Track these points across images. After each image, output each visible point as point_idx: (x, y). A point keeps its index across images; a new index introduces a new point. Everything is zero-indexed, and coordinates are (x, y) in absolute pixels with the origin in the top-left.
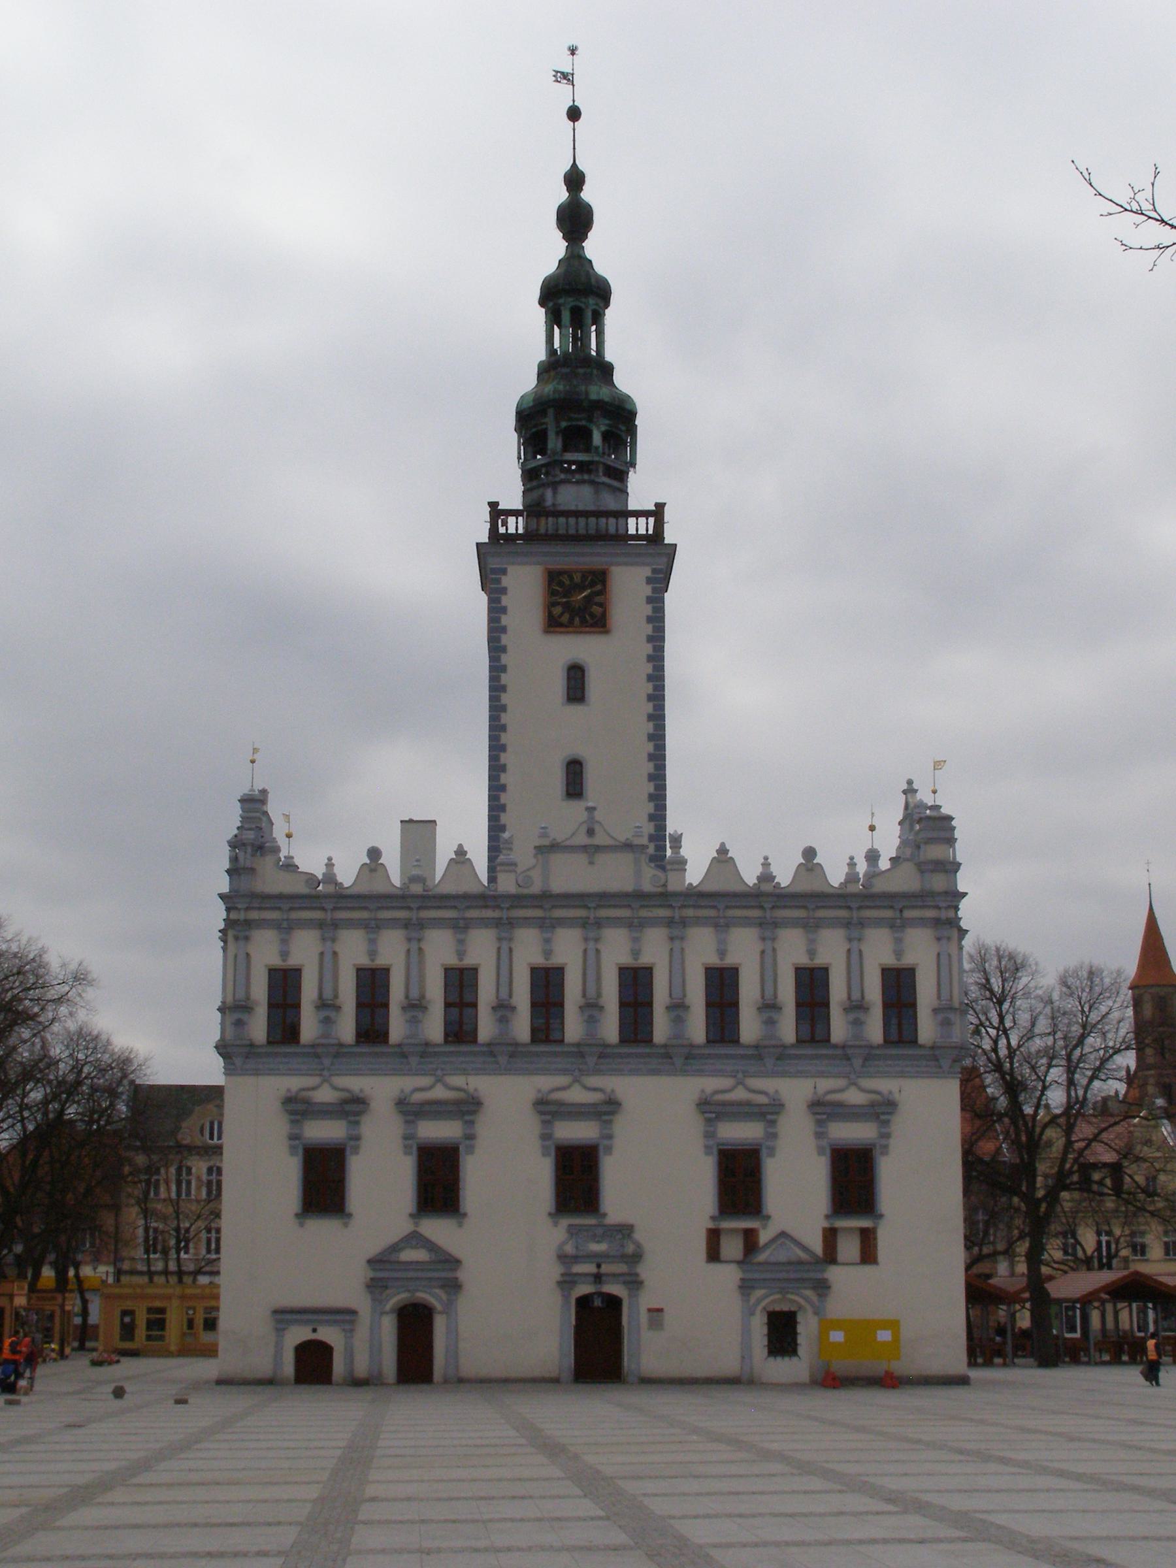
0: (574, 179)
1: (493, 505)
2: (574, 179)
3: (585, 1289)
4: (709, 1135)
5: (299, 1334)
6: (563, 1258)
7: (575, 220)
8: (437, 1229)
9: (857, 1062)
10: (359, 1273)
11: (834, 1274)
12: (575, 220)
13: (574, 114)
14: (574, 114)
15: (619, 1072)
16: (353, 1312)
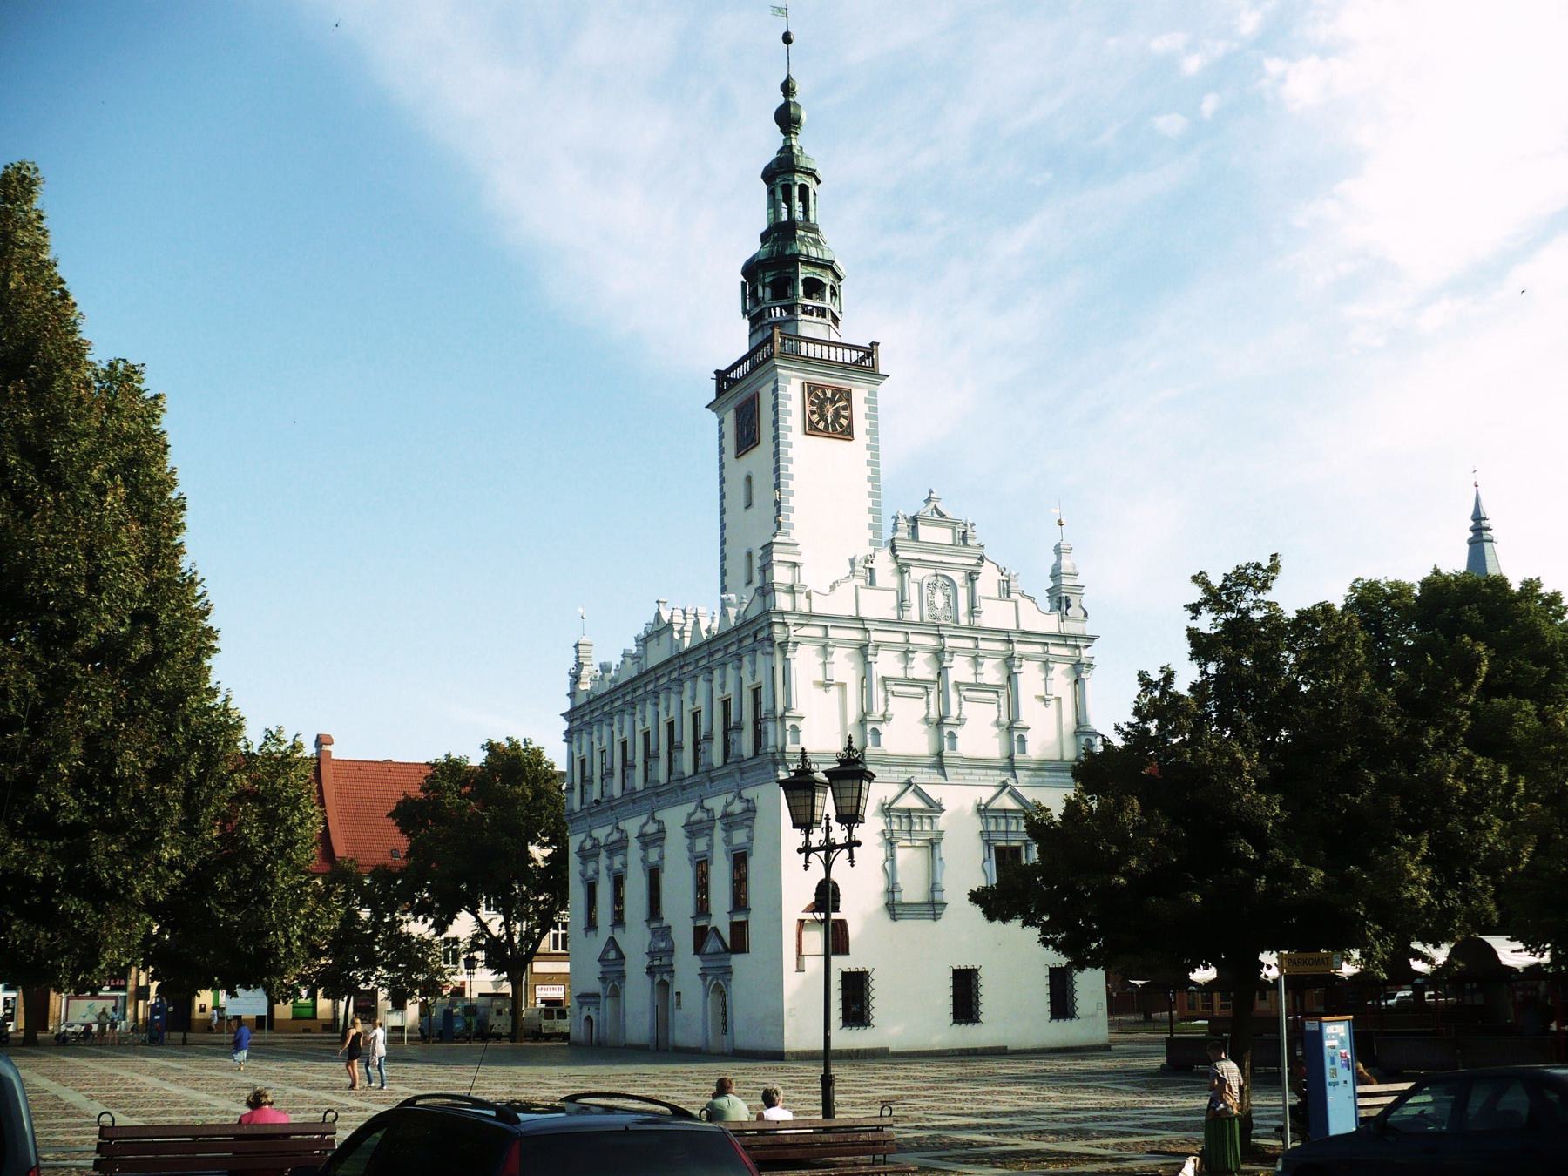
0: (787, 88)
1: (717, 372)
2: (787, 88)
3: (658, 978)
4: (691, 849)
5: (585, 1012)
6: (650, 953)
7: (787, 119)
8: (619, 935)
9: (738, 776)
10: (598, 967)
11: (736, 960)
12: (787, 119)
13: (787, 39)
14: (787, 39)
15: (666, 807)
16: (597, 996)
